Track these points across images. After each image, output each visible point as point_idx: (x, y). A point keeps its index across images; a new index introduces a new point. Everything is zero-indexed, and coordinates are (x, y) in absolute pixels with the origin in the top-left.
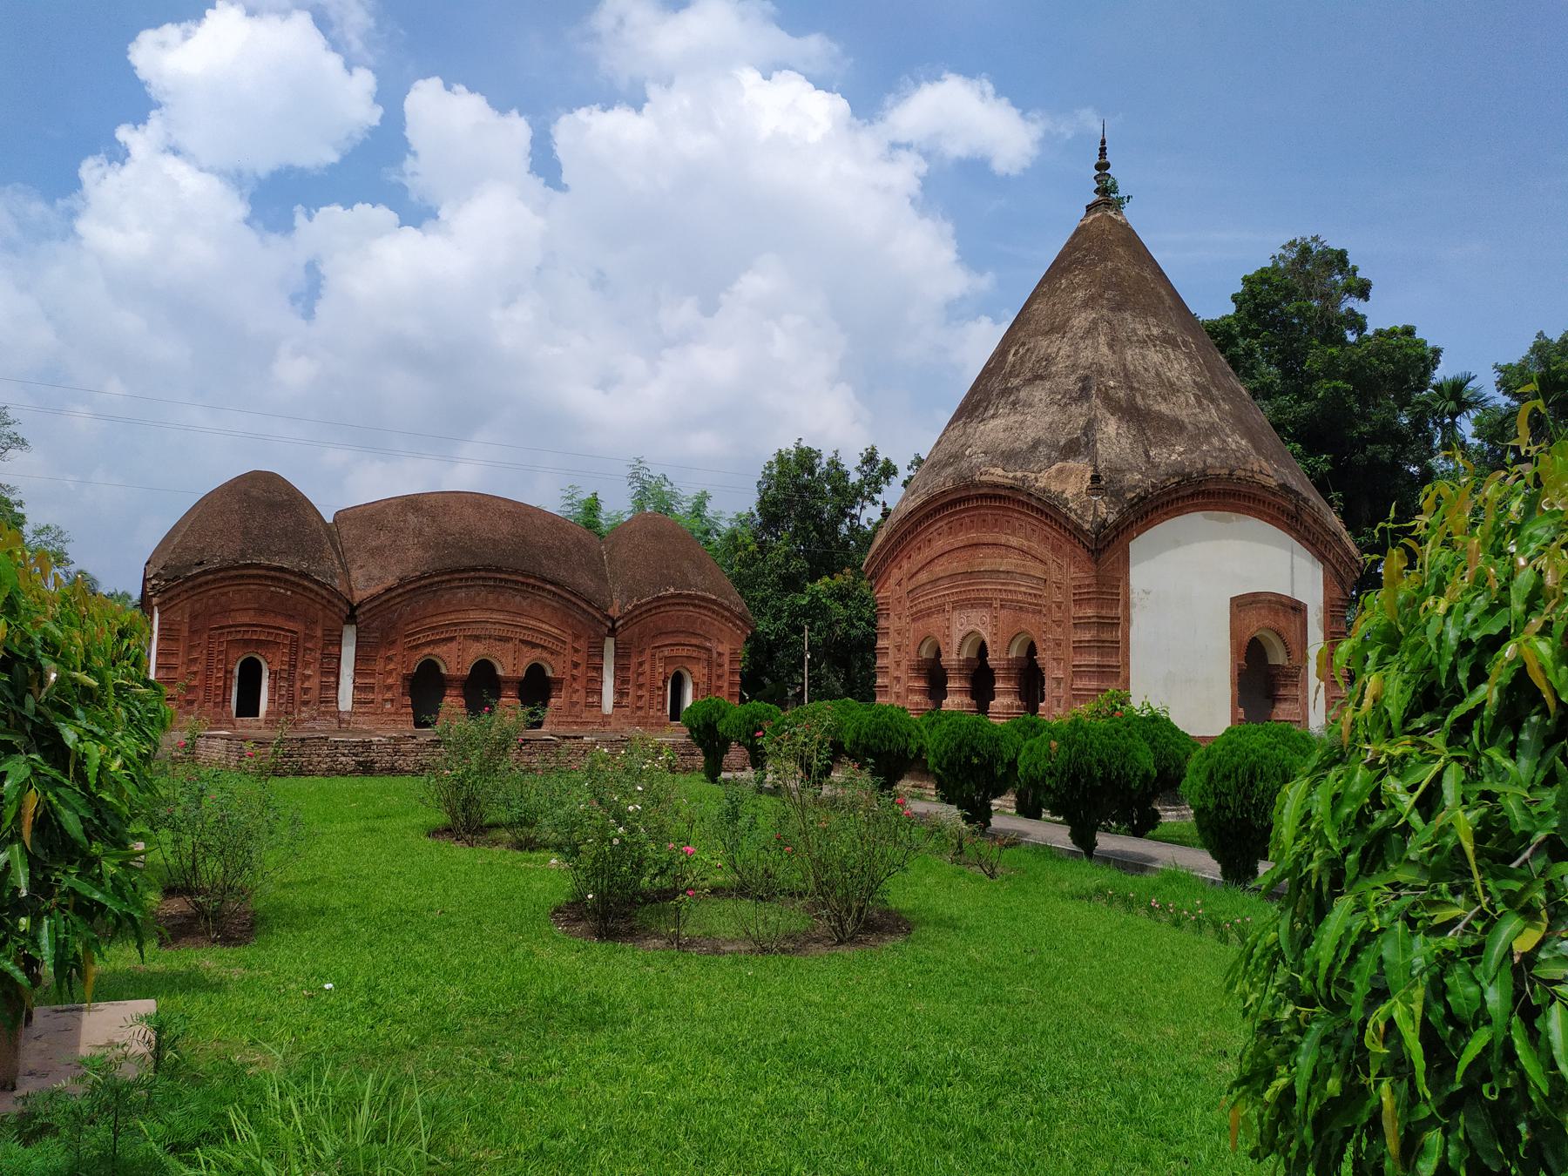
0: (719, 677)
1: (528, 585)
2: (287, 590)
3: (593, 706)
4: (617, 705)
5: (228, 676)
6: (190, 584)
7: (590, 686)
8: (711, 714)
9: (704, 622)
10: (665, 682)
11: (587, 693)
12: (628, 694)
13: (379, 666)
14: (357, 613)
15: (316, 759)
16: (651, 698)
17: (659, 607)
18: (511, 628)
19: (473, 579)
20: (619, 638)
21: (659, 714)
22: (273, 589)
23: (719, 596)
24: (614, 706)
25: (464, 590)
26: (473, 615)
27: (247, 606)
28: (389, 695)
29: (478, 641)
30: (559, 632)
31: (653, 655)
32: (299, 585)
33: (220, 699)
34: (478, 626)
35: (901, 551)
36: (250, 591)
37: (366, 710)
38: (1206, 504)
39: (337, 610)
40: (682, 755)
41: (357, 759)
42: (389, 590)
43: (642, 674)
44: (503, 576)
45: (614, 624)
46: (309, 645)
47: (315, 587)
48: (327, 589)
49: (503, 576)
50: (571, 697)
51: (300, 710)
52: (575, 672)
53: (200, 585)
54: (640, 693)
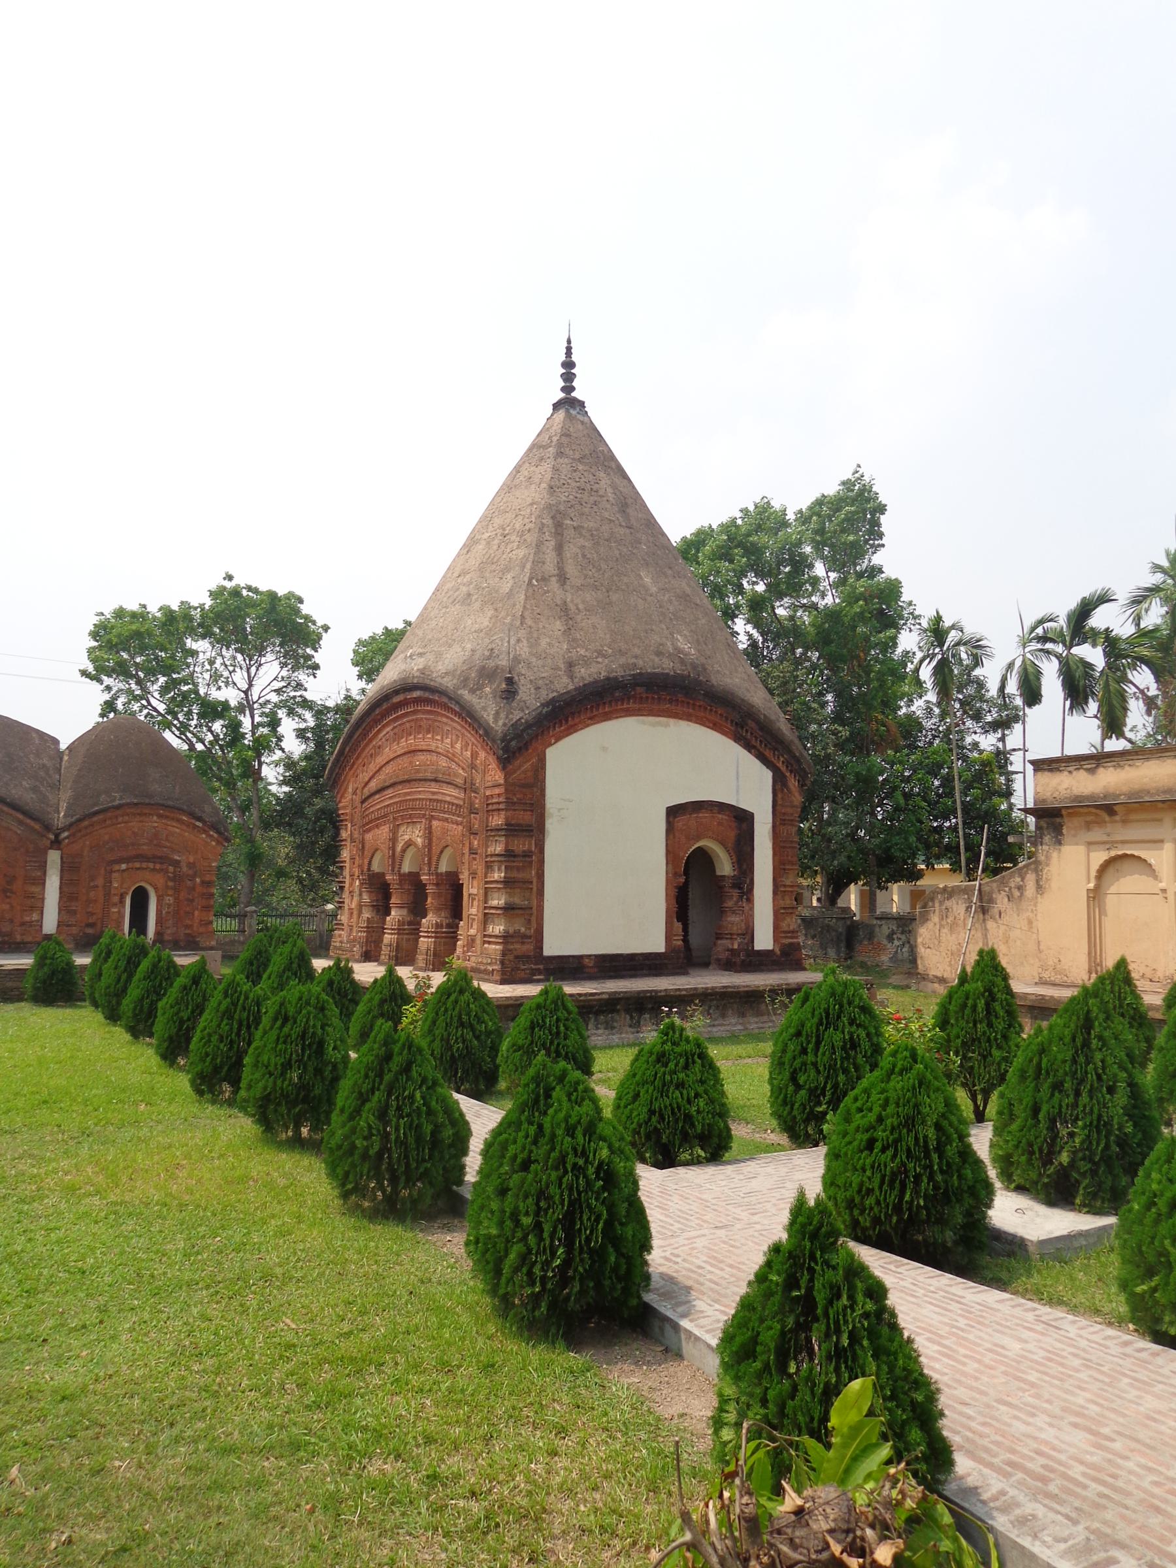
17: (116, 817)
35: (357, 758)
38: (639, 710)
45: (57, 836)
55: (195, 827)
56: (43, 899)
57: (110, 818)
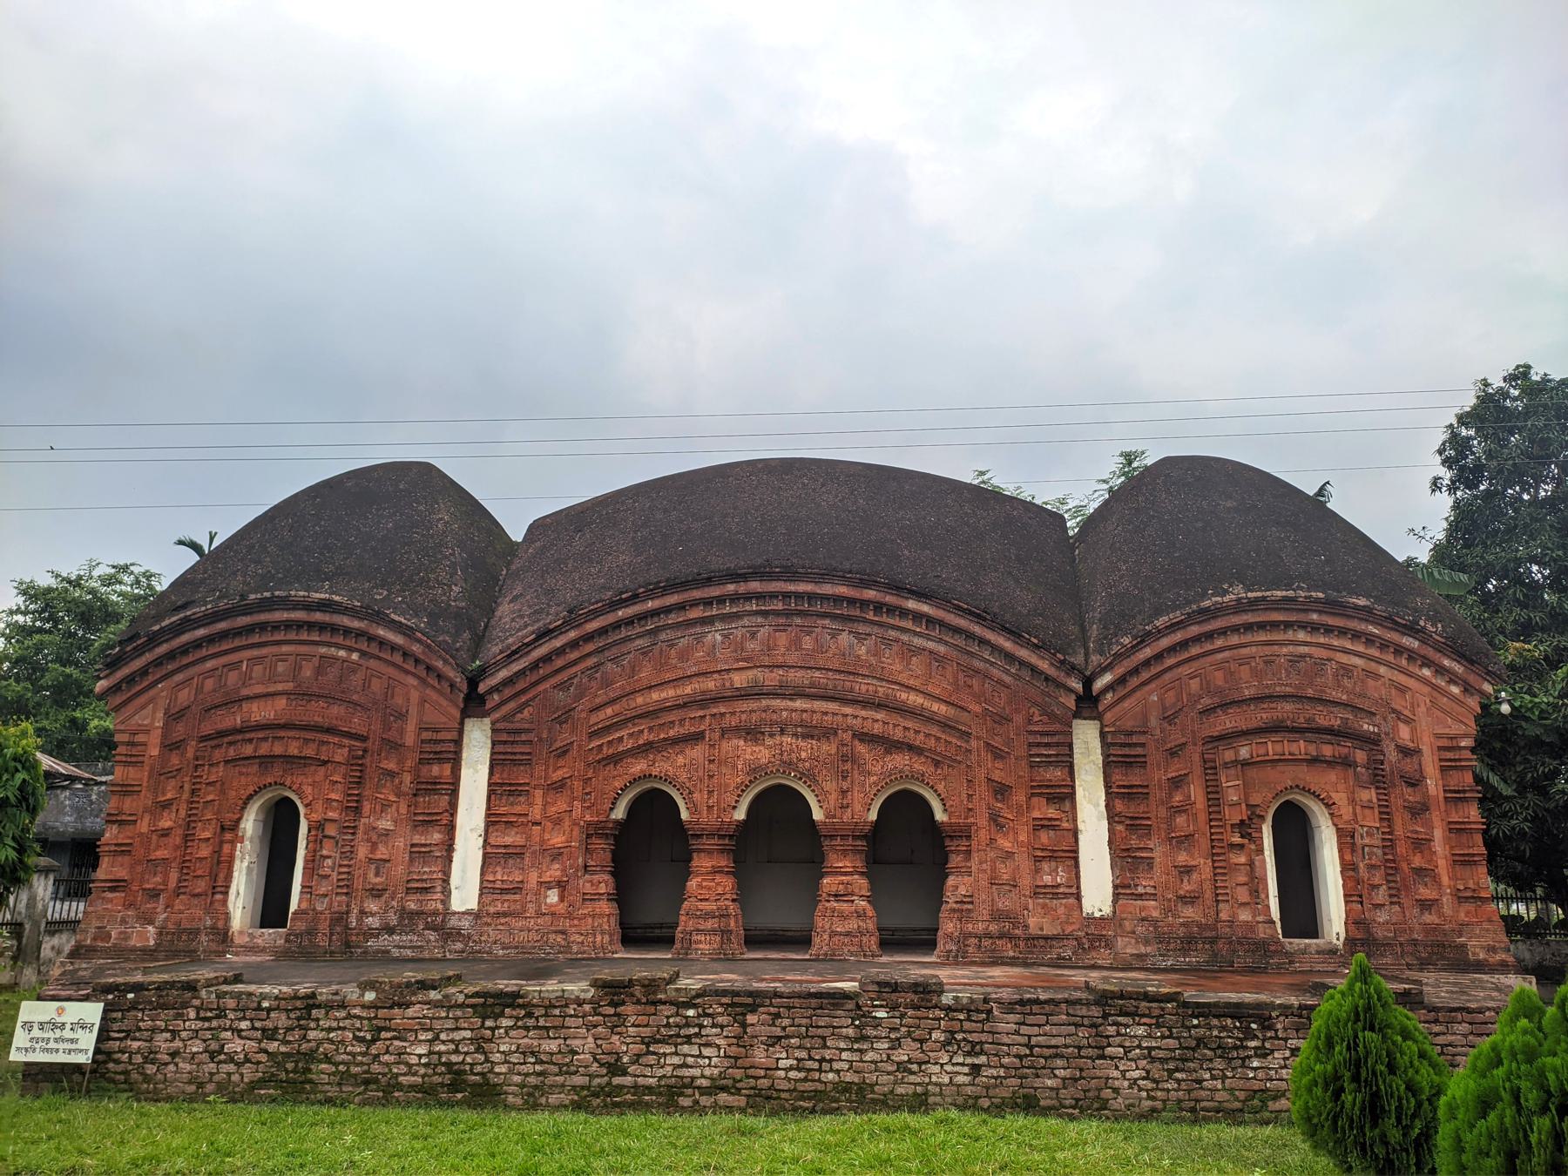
0: (1419, 811)
1: (864, 604)
2: (350, 650)
3: (1056, 896)
6: (163, 649)
9: (1347, 670)
11: (1038, 859)
12: (1151, 866)
14: (482, 688)
16: (1220, 870)
17: (1209, 636)
19: (735, 598)
20: (1108, 716)
22: (323, 650)
25: (719, 626)
27: (271, 689)
28: (554, 871)
29: (756, 741)
30: (951, 712)
32: (371, 638)
33: (201, 886)
36: (282, 658)
44: (802, 587)
47: (399, 639)
49: (802, 587)
54: (1182, 858)
55: (1399, 650)
56: (1075, 833)
57: (1197, 639)
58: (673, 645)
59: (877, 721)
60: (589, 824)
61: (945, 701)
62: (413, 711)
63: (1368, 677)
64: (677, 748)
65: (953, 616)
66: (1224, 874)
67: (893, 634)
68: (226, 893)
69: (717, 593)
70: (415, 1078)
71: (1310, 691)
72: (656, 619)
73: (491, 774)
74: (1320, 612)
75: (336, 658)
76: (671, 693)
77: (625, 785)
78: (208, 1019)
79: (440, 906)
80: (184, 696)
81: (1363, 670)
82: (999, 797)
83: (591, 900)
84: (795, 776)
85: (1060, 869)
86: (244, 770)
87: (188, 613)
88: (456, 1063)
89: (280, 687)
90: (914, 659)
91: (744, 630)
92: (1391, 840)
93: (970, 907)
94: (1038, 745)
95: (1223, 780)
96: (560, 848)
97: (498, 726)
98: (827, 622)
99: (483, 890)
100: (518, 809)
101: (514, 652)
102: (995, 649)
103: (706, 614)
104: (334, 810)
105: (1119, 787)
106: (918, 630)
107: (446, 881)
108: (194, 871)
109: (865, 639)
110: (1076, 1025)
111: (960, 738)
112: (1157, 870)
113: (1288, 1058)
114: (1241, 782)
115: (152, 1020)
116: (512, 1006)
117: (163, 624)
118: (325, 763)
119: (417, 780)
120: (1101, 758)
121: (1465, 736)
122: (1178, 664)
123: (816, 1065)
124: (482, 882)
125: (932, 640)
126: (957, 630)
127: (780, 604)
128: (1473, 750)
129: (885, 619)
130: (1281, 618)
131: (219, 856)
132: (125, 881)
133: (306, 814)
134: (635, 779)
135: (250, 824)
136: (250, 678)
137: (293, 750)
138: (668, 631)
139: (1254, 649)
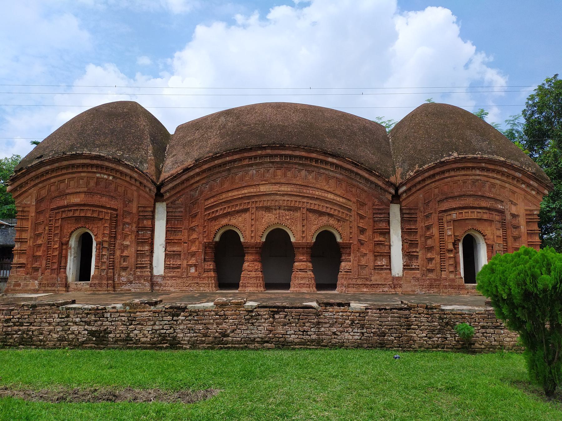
0: (516, 239)
1: (311, 159)
2: (109, 175)
3: (382, 269)
4: (406, 267)
5: (64, 247)
6: (33, 174)
7: (378, 249)
8: (534, 277)
9: (493, 185)
10: (455, 244)
11: (375, 256)
12: (417, 257)
13: (183, 236)
15: (47, 328)
16: (442, 260)
17: (443, 172)
18: (298, 199)
20: (404, 203)
21: (452, 276)
22: (98, 175)
23: (508, 158)
24: (404, 269)
26: (263, 189)
27: (78, 190)
28: (193, 261)
30: (344, 201)
31: (440, 219)
32: (117, 171)
33: (55, 266)
34: (268, 198)
37: (174, 274)
39: (148, 190)
40: (483, 327)
41: (89, 328)
42: (186, 170)
43: (430, 237)
46: (127, 220)
48: (136, 172)
50: (359, 260)
51: (119, 275)
52: (362, 237)
53: (42, 175)
54: (429, 255)
55: (514, 178)
56: (390, 246)
57: (438, 174)
58: (237, 175)
59: (315, 205)
60: (205, 243)
61: (342, 197)
62: (135, 200)
63: (501, 188)
64: (239, 214)
65: (346, 164)
66: (445, 261)
67: (322, 171)
68: (65, 269)
69: (254, 154)
70: (147, 339)
71: (480, 193)
72: (230, 164)
73: (167, 223)
74: (486, 163)
75: (103, 179)
76: (236, 193)
77: (219, 228)
78: (63, 318)
79: (149, 274)
80: (44, 193)
81: (500, 185)
82: (362, 233)
83: (207, 271)
84: (285, 225)
85: (384, 259)
86: (69, 222)
87: (42, 160)
88: (163, 333)
89: (82, 190)
90: (330, 181)
91: (264, 169)
92: (506, 248)
93: (350, 273)
94: (377, 214)
95: (446, 226)
96: (195, 252)
97: (169, 205)
98: (297, 166)
99: (166, 268)
100: (177, 238)
101: (175, 177)
102: (362, 177)
103: (249, 163)
104: (107, 237)
105: (406, 229)
106: (332, 169)
107: (151, 264)
108: (52, 260)
109: (312, 173)
110: (400, 317)
111: (348, 211)
112: (419, 260)
113: (479, 329)
114: (452, 227)
115: (41, 319)
116: (184, 311)
117: (33, 164)
118: (101, 219)
119: (137, 227)
120: (400, 218)
121: (536, 210)
122: (431, 183)
123: (302, 333)
124: (165, 264)
125: (337, 174)
126: (346, 169)
127: (279, 159)
128: (538, 215)
129: (319, 165)
130: (471, 165)
131: (62, 255)
132: (24, 264)
133: (95, 239)
134: (223, 226)
135: (73, 243)
136: (69, 186)
137: (89, 215)
138: (235, 169)
139: (459, 177)
